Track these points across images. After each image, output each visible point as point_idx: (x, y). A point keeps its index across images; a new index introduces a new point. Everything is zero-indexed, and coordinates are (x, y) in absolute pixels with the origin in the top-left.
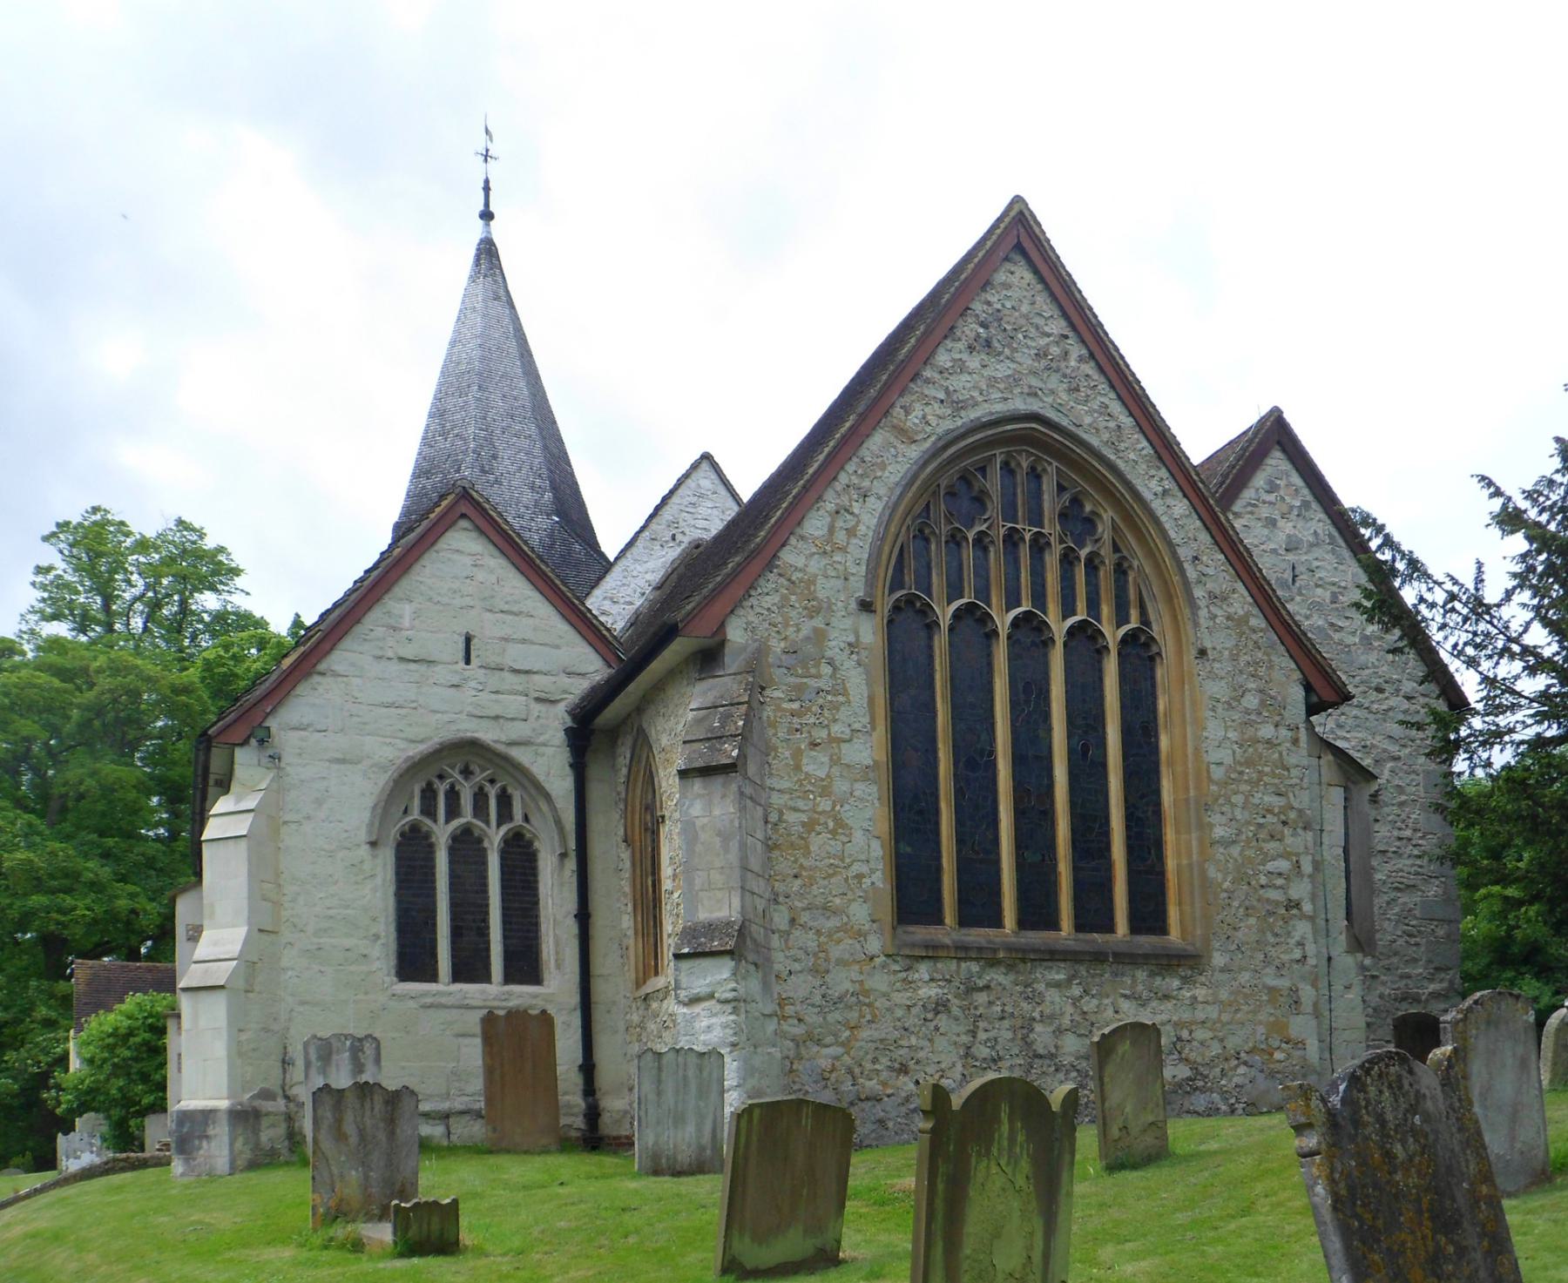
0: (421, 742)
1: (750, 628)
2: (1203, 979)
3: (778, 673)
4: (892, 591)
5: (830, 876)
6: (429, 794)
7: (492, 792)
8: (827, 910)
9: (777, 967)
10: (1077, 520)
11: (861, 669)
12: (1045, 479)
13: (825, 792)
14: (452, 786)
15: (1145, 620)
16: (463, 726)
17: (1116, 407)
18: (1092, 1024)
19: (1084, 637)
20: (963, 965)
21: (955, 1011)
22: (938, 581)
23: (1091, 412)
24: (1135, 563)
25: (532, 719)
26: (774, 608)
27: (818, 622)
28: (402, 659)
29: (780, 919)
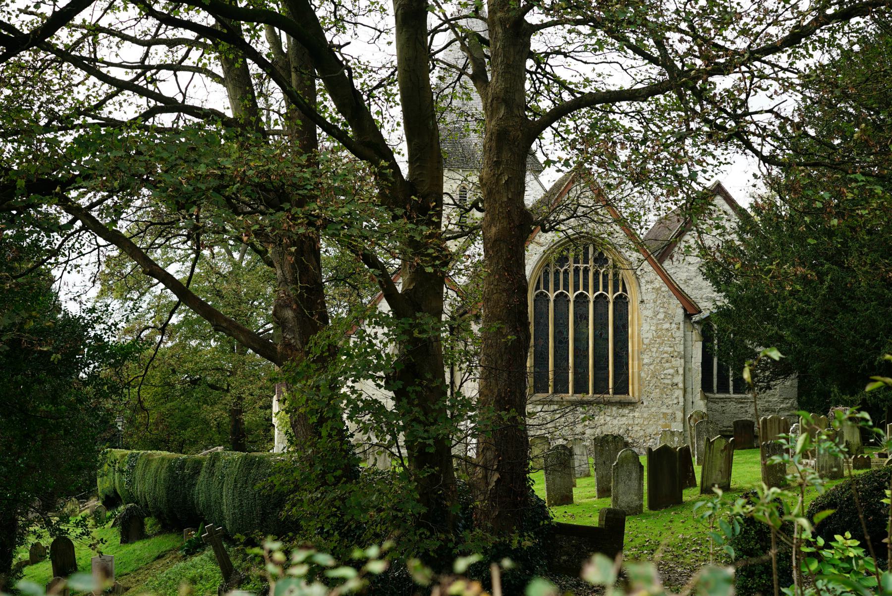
4: (536, 290)
15: (625, 290)
19: (601, 300)
22: (551, 286)
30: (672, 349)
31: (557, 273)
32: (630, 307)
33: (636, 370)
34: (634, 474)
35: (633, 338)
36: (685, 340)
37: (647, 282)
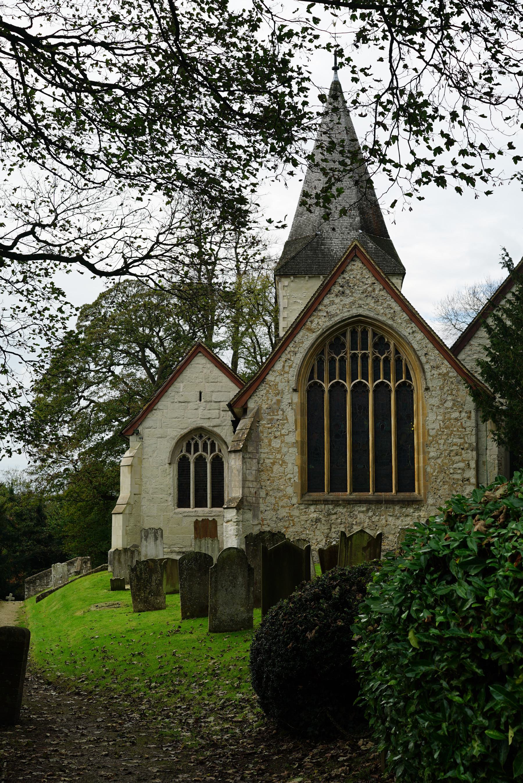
2: (423, 508)
4: (309, 381)
6: (189, 445)
9: (261, 509)
14: (196, 442)
15: (409, 377)
16: (199, 422)
17: (394, 305)
21: (323, 522)
22: (326, 375)
25: (221, 418)
27: (279, 397)
29: (263, 494)
30: (462, 441)
31: (332, 361)
32: (415, 396)
33: (421, 464)
34: (240, 579)
35: (418, 429)
37: (433, 367)
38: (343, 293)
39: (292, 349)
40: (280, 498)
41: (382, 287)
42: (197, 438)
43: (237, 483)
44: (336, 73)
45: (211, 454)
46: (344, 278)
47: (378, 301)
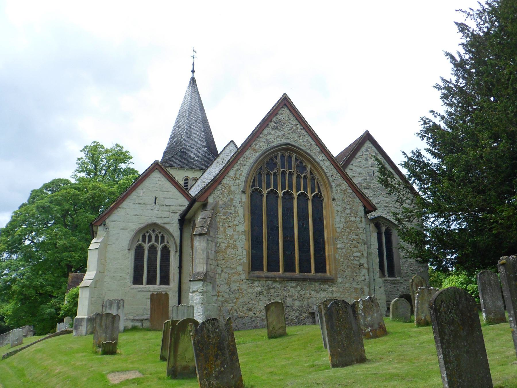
0: (143, 224)
1: (214, 199)
2: (335, 285)
3: (221, 209)
4: (252, 187)
5: (232, 259)
6: (144, 237)
7: (160, 236)
8: (231, 268)
9: (218, 283)
10: (301, 167)
11: (242, 208)
12: (292, 158)
13: (232, 238)
14: (150, 234)
15: (319, 191)
16: (153, 220)
18: (303, 298)
19: (303, 197)
20: (267, 282)
21: (265, 294)
22: (264, 185)
23: (304, 141)
24: (317, 177)
26: (221, 194)
27: (231, 197)
28: (139, 204)
29: (219, 270)
31: (268, 174)
36: (366, 231)
38: (277, 128)
39: (242, 162)
40: (232, 275)
41: (302, 127)
42: (151, 232)
43: (201, 261)
44: (193, 74)
45: (161, 244)
46: (277, 118)
47: (300, 136)
